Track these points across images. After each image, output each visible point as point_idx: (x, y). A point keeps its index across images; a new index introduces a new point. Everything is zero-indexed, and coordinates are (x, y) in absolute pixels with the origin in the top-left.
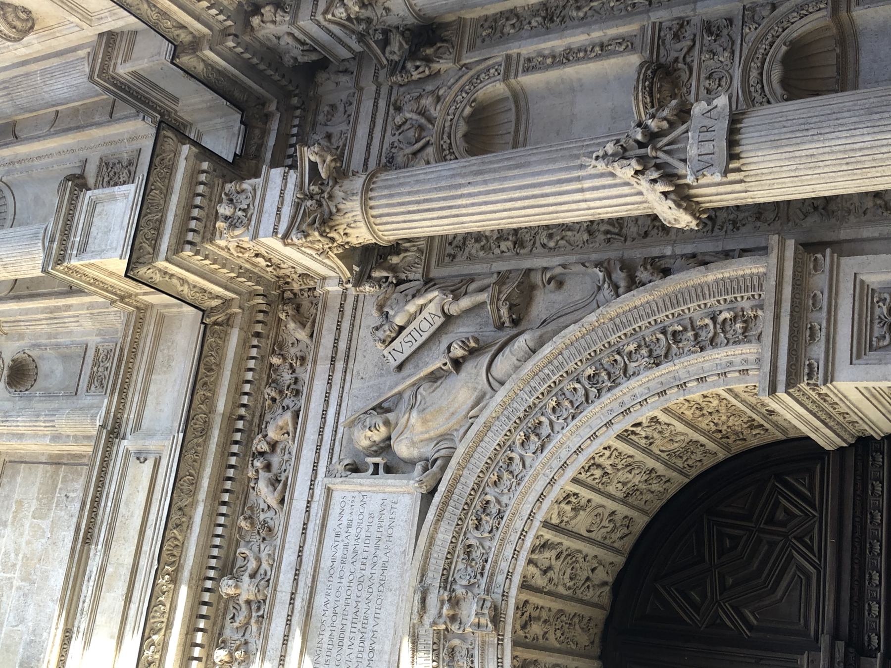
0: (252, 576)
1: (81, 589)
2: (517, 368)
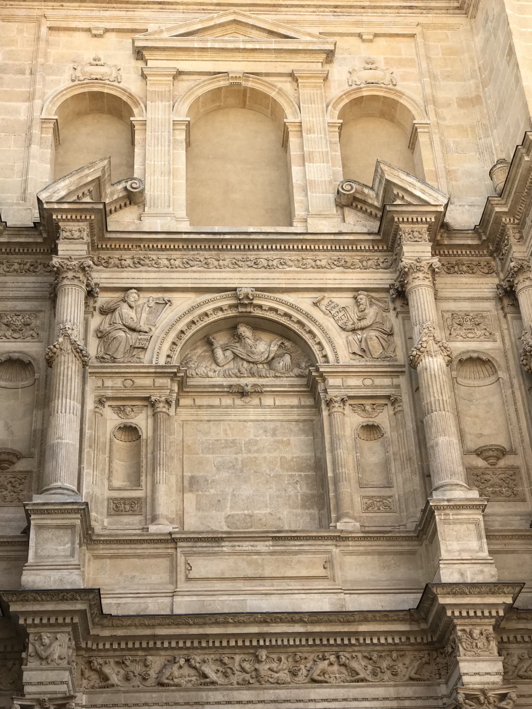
0: (270, 669)
1: (246, 541)
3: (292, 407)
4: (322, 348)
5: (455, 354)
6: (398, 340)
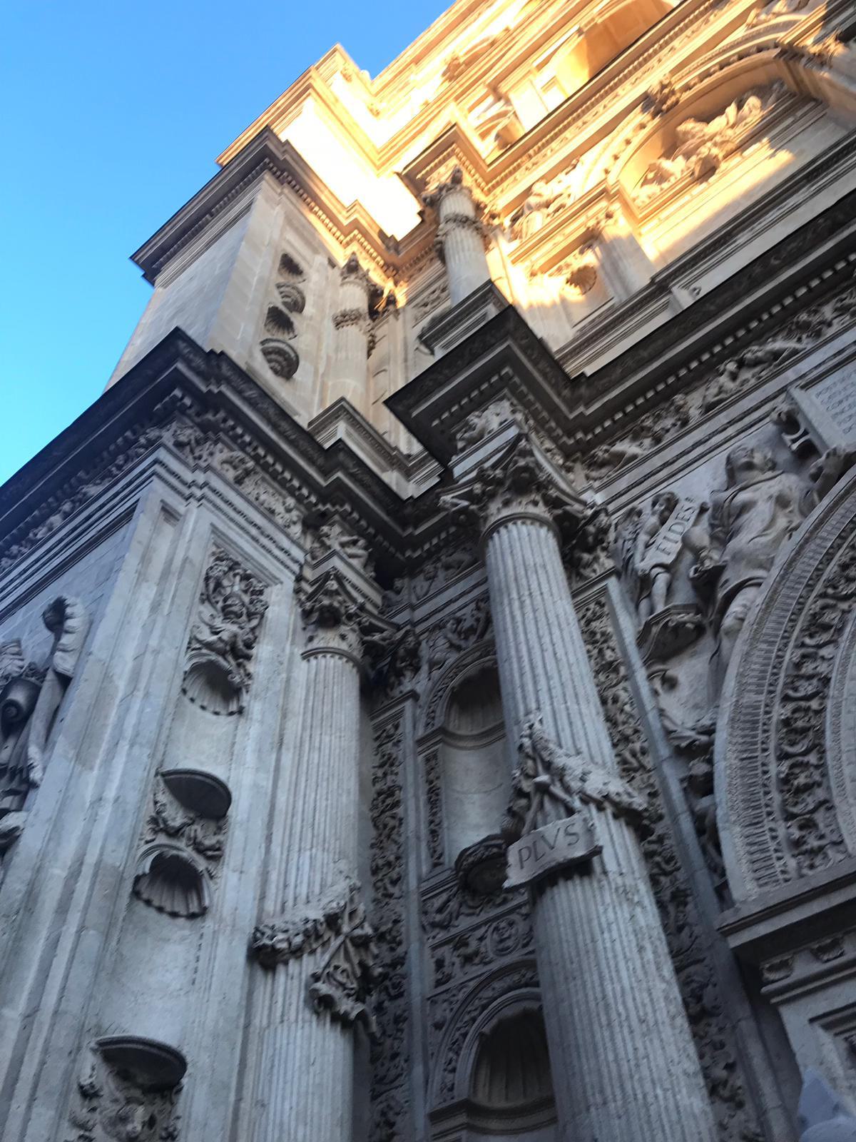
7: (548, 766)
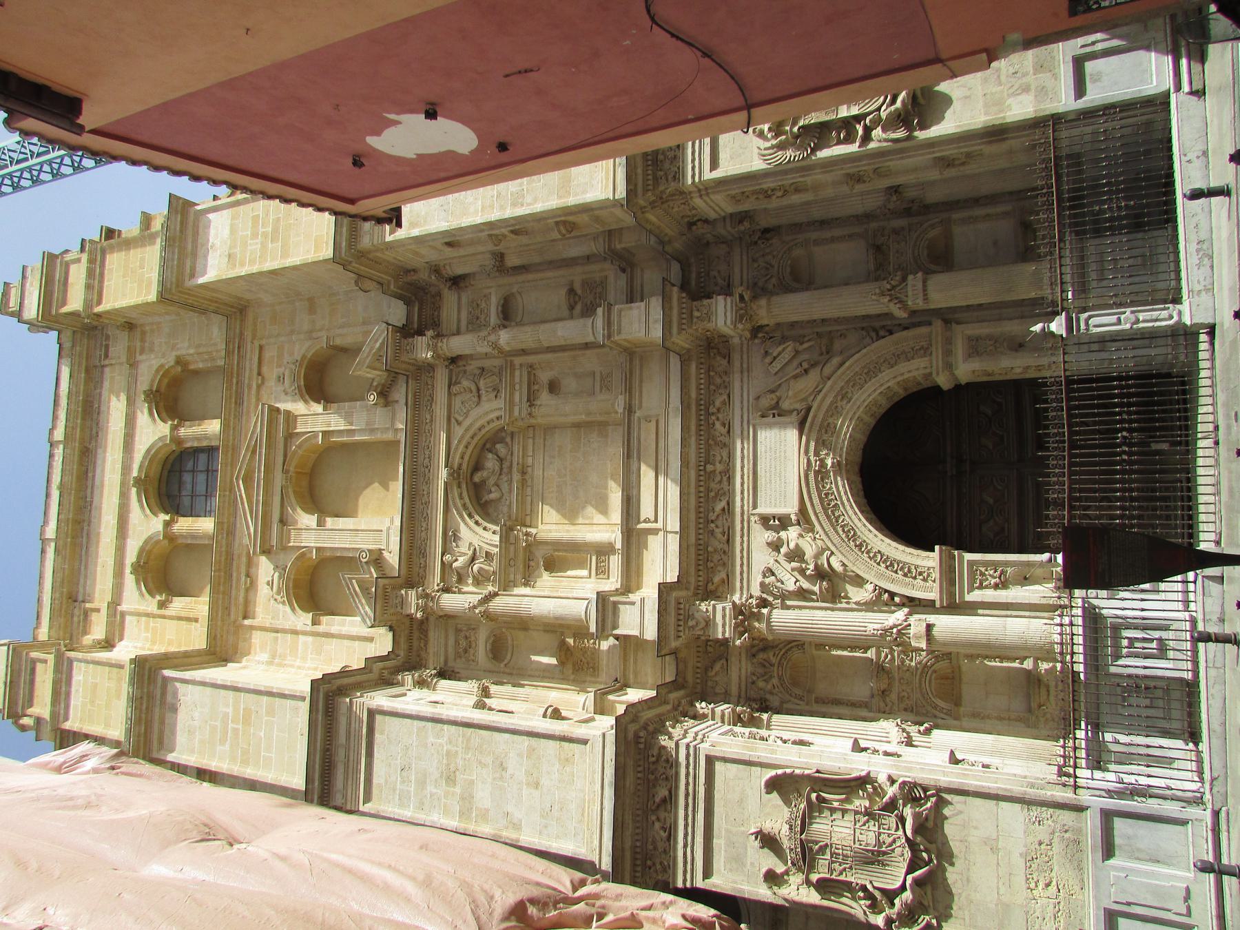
2: (835, 372)
3: (534, 443)
4: (492, 420)
5: (499, 322)
6: (487, 363)
7: (892, 628)
